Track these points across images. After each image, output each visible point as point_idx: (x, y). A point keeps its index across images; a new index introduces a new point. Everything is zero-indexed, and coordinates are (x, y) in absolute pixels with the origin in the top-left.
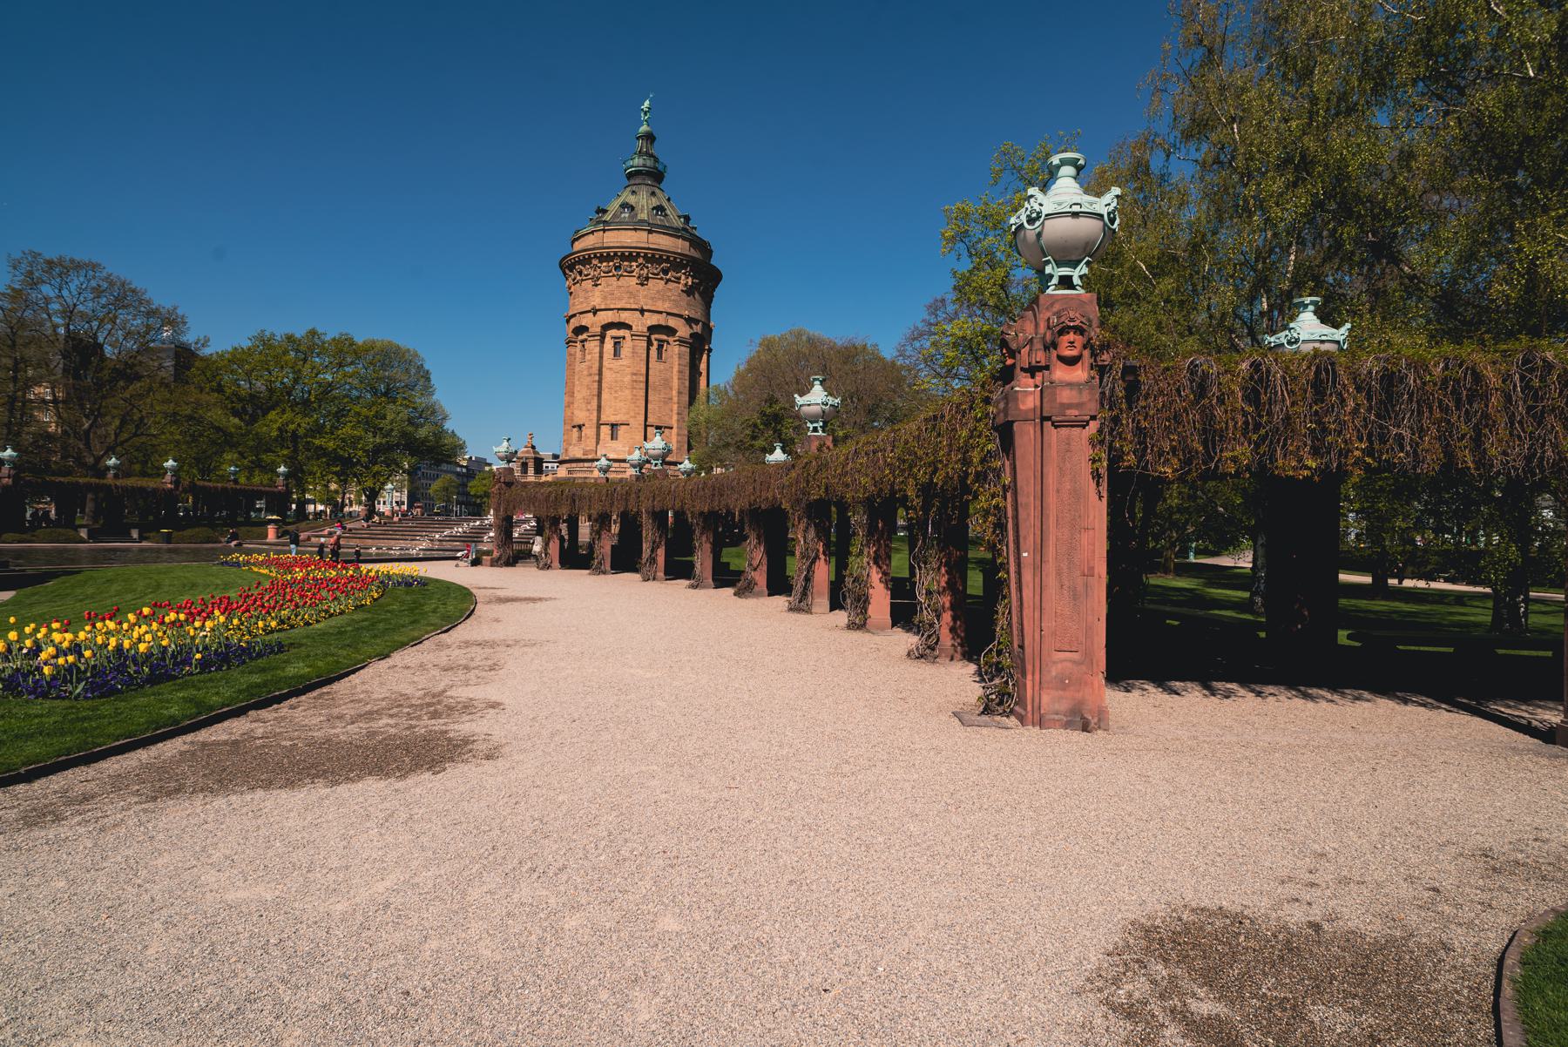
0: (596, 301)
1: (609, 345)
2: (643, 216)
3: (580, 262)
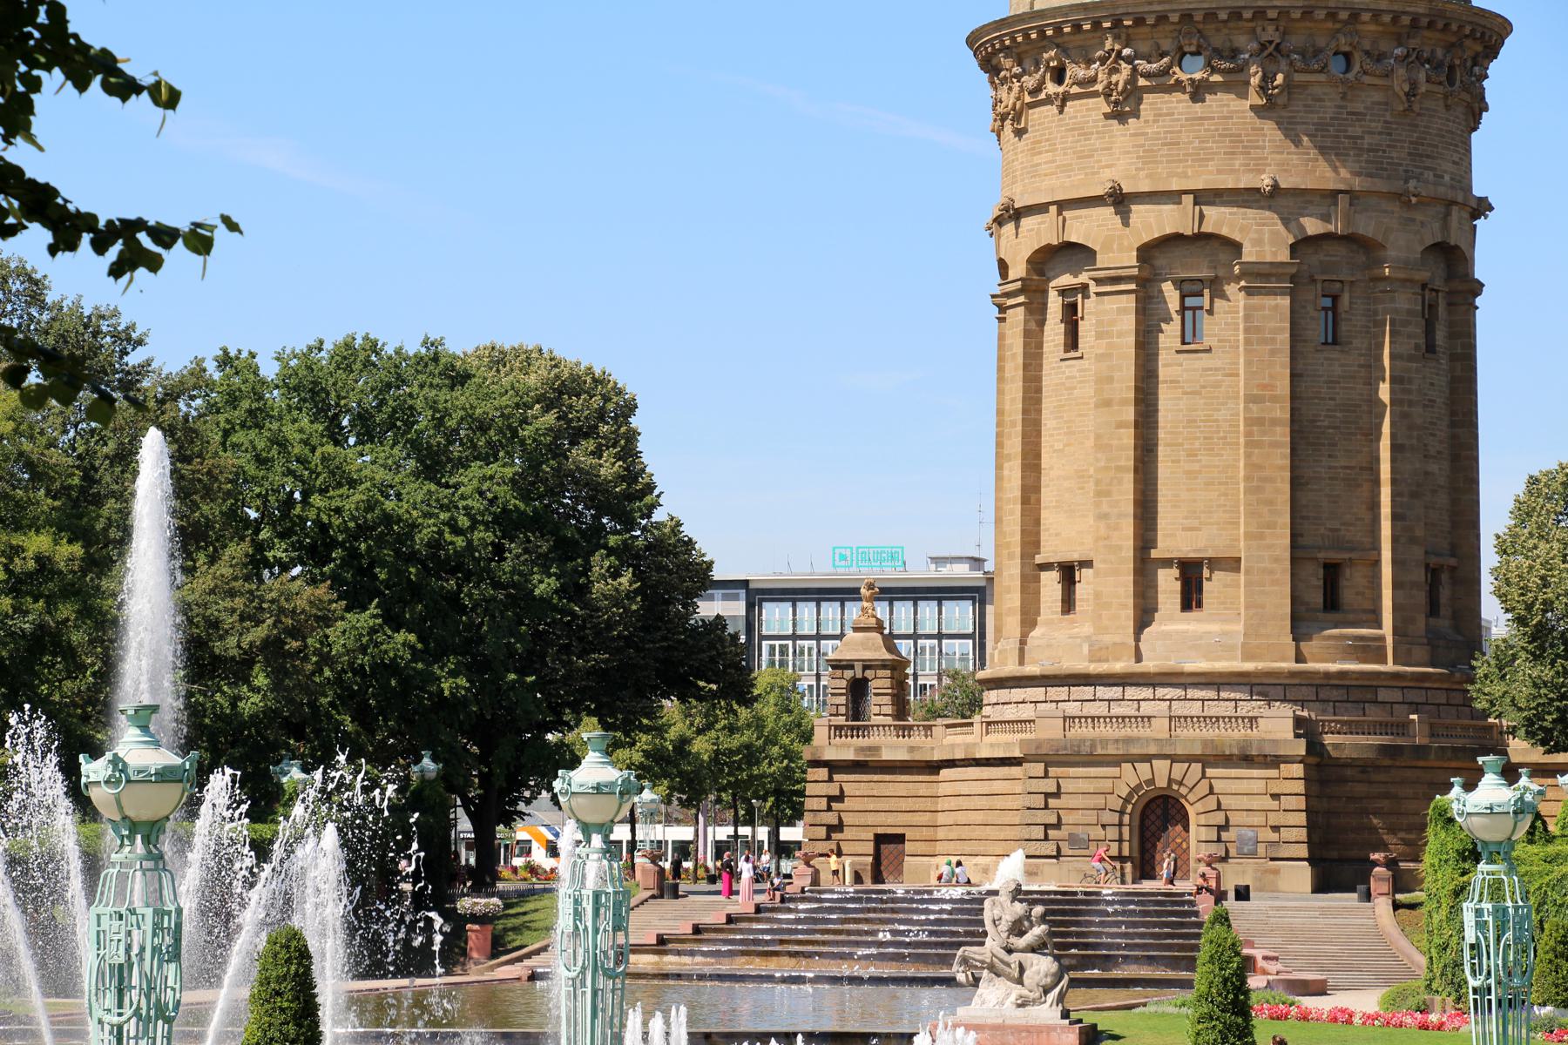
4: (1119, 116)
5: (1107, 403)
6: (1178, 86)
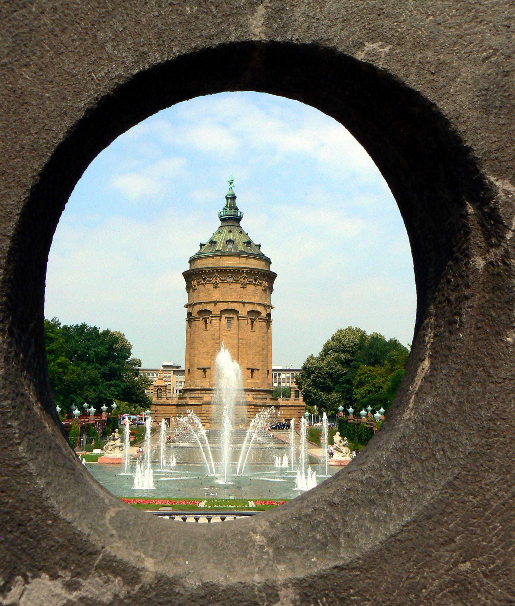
0: (216, 296)
1: (224, 321)
2: (241, 248)
3: (205, 273)
4: (216, 287)
5: (214, 339)
6: (227, 282)
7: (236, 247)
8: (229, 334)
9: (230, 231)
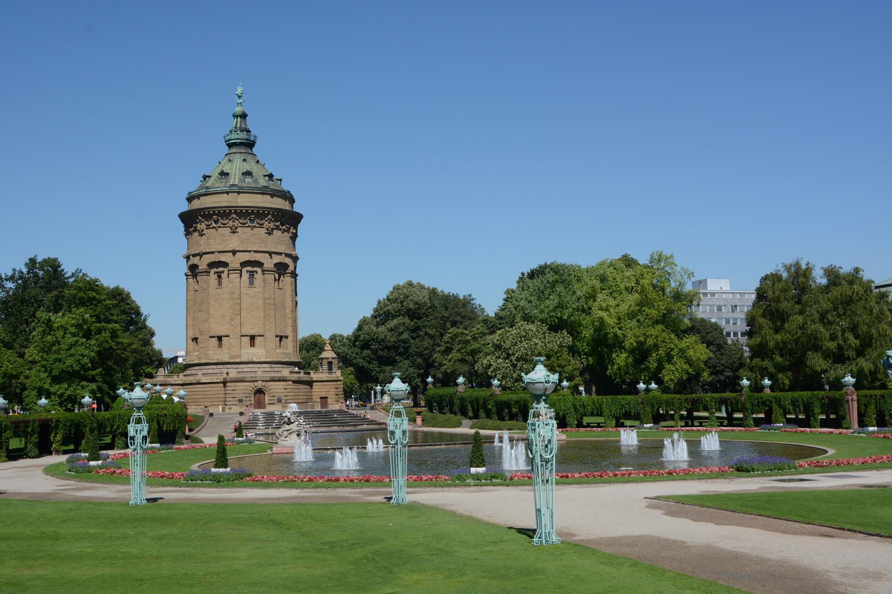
0: (234, 243)
1: (246, 276)
2: (263, 182)
3: (219, 214)
4: (234, 232)
7: (256, 181)
8: (252, 291)
9: (244, 160)
